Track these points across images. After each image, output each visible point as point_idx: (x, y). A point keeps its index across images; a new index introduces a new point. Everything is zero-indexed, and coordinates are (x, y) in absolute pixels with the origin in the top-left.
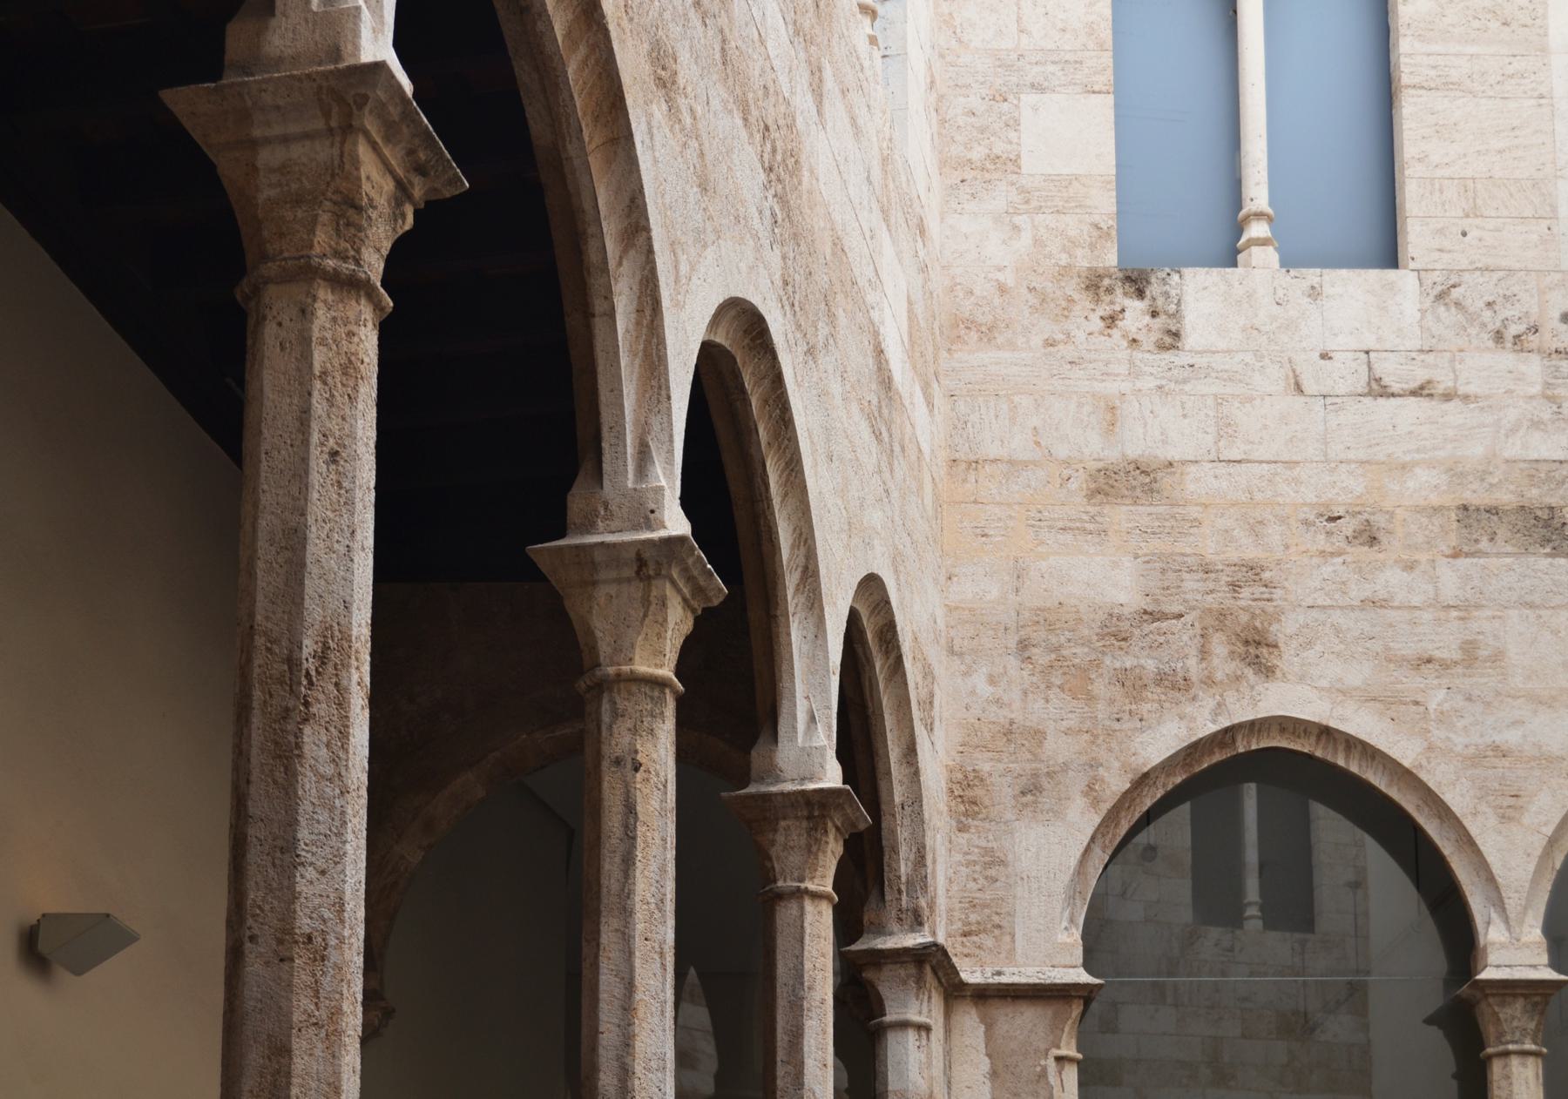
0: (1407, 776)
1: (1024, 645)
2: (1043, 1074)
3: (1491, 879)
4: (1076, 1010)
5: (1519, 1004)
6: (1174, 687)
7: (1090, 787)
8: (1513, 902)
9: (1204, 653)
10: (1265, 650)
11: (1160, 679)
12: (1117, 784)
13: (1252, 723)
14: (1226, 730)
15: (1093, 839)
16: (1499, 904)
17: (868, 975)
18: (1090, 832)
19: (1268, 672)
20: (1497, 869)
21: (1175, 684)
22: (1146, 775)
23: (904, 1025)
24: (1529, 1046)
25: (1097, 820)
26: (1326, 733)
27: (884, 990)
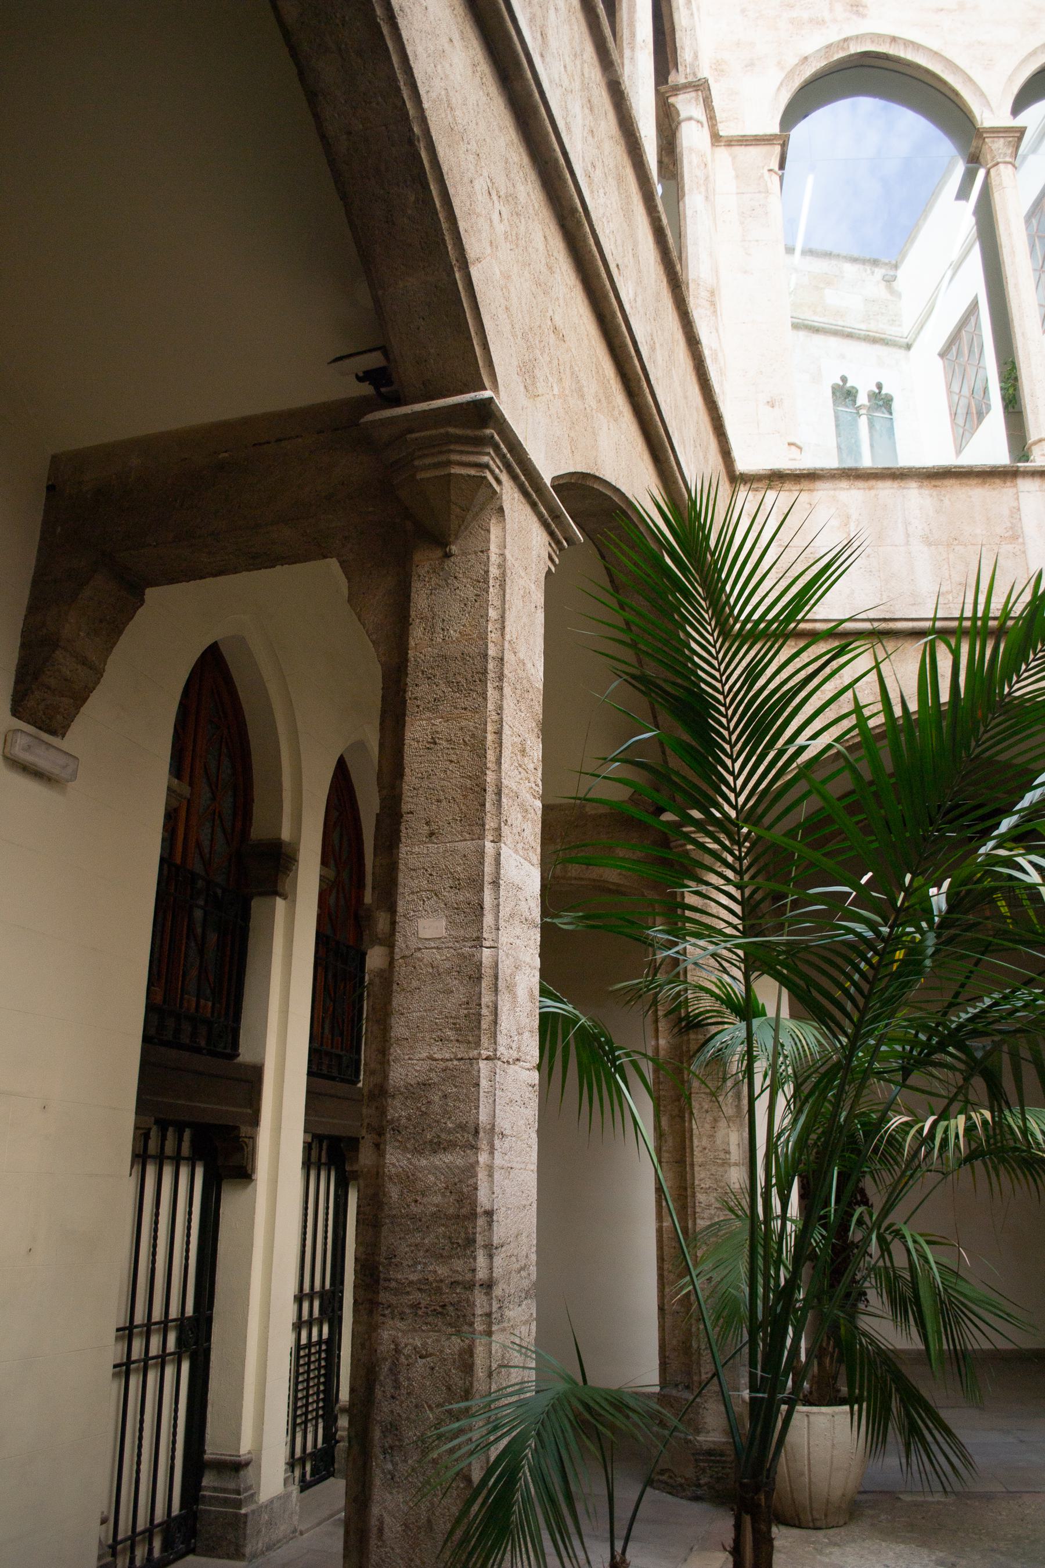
0: (936, 55)
1: (743, 11)
2: (762, 176)
3: (982, 95)
4: (777, 149)
5: (1002, 140)
6: (818, 23)
7: (779, 63)
8: (993, 104)
9: (831, 10)
10: (861, 9)
11: (811, 21)
12: (792, 61)
13: (857, 37)
14: (846, 40)
15: (781, 84)
16: (988, 104)
17: (671, 100)
18: (780, 81)
19: (864, 16)
20: (984, 89)
21: (820, 23)
22: (806, 58)
23: (690, 119)
24: (1008, 159)
25: (783, 75)
26: (894, 39)
27: (679, 107)
